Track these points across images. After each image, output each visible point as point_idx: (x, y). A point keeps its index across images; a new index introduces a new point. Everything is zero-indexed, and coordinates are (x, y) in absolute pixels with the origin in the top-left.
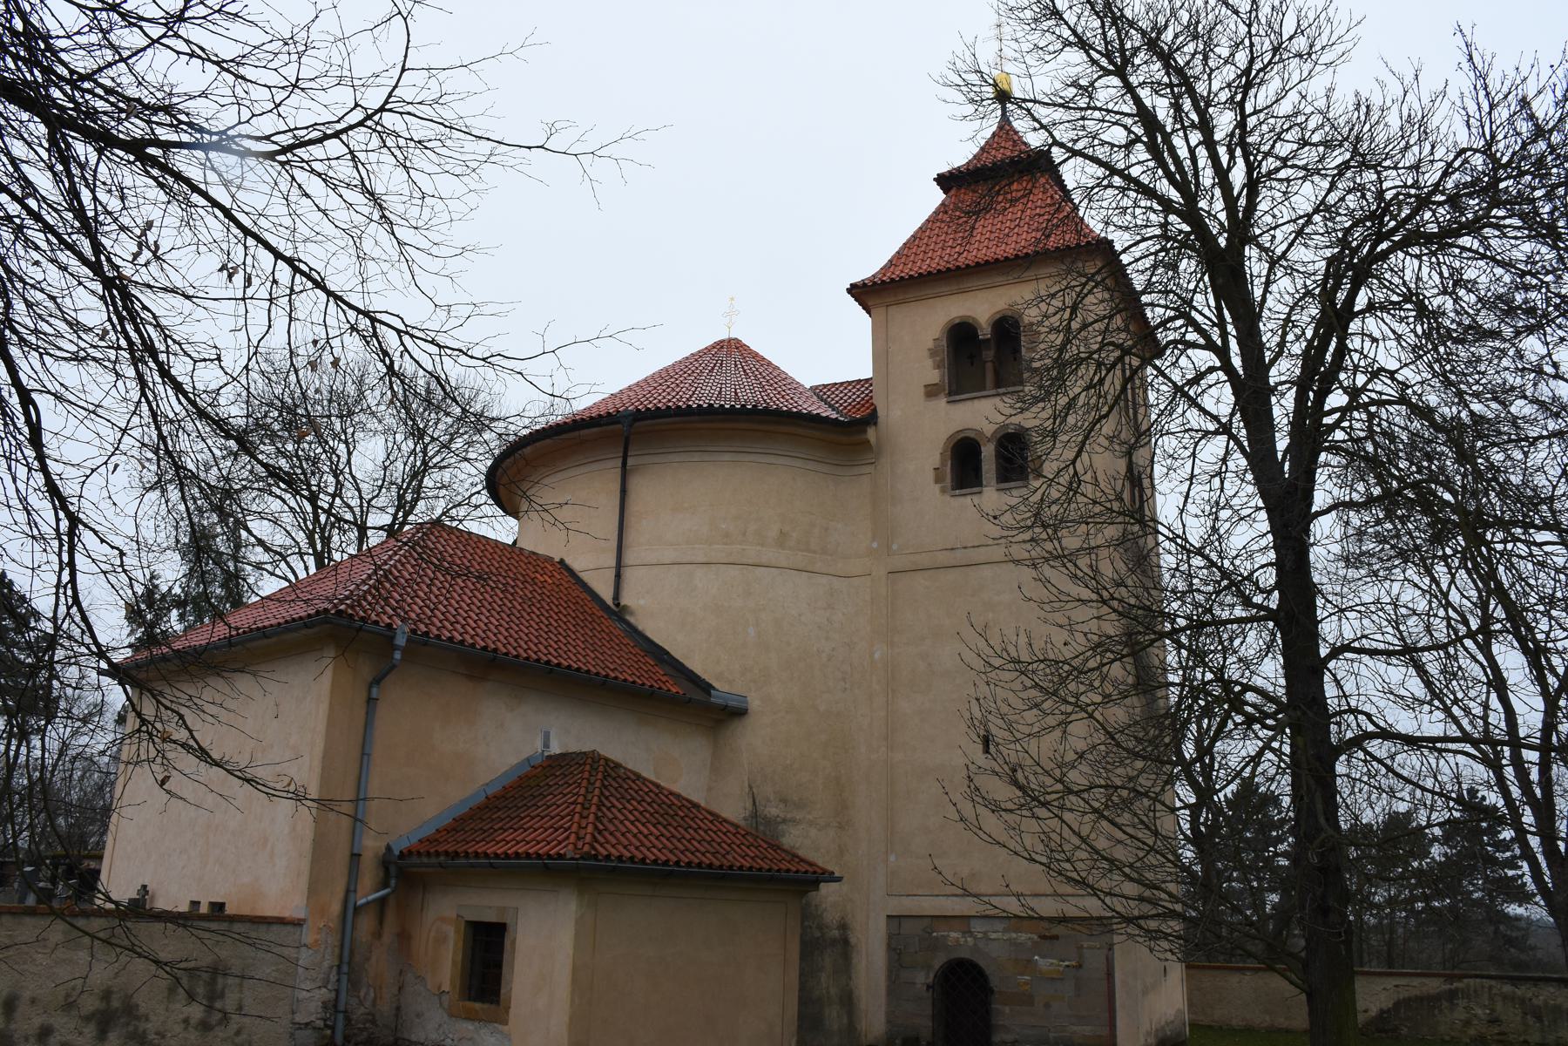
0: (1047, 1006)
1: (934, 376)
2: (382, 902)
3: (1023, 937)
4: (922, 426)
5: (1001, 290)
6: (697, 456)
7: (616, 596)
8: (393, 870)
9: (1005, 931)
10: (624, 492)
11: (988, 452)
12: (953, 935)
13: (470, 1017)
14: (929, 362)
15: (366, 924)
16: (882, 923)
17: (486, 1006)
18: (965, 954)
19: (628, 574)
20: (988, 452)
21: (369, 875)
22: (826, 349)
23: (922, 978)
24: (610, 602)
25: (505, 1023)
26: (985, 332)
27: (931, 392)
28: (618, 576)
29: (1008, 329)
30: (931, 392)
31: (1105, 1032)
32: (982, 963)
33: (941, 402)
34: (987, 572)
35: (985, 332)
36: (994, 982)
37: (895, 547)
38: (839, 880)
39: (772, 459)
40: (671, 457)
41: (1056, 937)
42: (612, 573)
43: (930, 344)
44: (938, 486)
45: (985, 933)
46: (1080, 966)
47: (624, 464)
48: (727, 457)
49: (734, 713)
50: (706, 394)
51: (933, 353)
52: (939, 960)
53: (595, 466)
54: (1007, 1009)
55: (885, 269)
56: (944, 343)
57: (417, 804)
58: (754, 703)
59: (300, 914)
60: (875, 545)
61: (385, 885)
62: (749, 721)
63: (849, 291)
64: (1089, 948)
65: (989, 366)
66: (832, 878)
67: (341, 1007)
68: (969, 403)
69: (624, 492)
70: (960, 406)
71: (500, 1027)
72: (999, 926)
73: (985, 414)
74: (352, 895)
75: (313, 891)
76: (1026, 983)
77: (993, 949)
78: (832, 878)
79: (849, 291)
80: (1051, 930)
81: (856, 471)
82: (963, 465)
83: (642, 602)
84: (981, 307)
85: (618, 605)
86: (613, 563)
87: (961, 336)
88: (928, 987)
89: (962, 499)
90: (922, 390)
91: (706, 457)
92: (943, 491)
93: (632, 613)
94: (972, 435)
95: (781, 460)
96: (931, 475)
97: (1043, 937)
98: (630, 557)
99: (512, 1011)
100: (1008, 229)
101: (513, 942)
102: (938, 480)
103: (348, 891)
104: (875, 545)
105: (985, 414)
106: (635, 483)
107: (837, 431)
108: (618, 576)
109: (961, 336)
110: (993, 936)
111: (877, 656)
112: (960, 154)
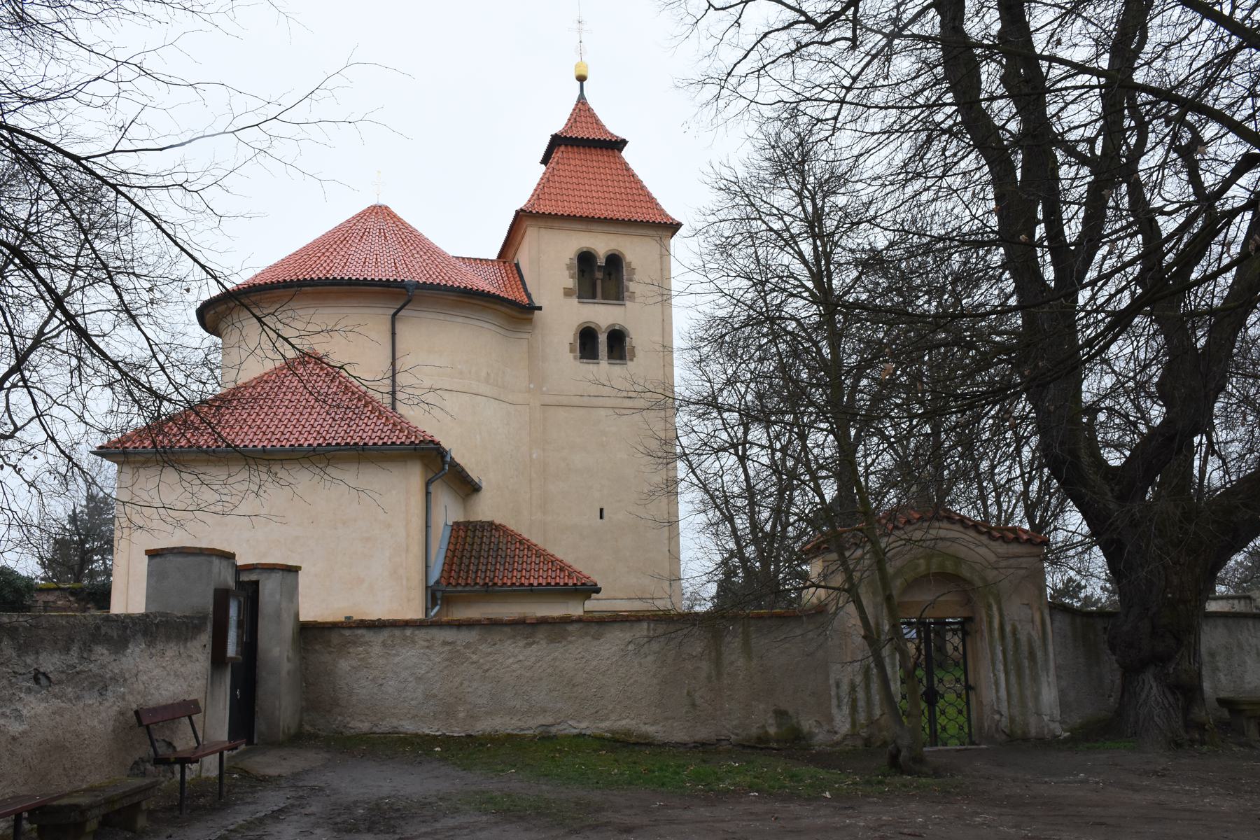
1: (571, 283)
4: (562, 313)
5: (611, 236)
6: (442, 317)
8: (439, 595)
10: (394, 334)
11: (603, 338)
20: (603, 338)
26: (601, 261)
27: (568, 293)
29: (615, 261)
30: (568, 293)
33: (574, 301)
34: (602, 412)
40: (424, 314)
43: (568, 261)
47: (394, 315)
48: (460, 320)
51: (569, 267)
58: (484, 485)
69: (394, 334)
73: (603, 315)
78: (598, 591)
82: (587, 341)
84: (601, 244)
87: (585, 260)
91: (448, 318)
92: (575, 358)
95: (486, 325)
96: (567, 348)
105: (603, 315)
106: (400, 328)
109: (585, 260)
111: (534, 456)
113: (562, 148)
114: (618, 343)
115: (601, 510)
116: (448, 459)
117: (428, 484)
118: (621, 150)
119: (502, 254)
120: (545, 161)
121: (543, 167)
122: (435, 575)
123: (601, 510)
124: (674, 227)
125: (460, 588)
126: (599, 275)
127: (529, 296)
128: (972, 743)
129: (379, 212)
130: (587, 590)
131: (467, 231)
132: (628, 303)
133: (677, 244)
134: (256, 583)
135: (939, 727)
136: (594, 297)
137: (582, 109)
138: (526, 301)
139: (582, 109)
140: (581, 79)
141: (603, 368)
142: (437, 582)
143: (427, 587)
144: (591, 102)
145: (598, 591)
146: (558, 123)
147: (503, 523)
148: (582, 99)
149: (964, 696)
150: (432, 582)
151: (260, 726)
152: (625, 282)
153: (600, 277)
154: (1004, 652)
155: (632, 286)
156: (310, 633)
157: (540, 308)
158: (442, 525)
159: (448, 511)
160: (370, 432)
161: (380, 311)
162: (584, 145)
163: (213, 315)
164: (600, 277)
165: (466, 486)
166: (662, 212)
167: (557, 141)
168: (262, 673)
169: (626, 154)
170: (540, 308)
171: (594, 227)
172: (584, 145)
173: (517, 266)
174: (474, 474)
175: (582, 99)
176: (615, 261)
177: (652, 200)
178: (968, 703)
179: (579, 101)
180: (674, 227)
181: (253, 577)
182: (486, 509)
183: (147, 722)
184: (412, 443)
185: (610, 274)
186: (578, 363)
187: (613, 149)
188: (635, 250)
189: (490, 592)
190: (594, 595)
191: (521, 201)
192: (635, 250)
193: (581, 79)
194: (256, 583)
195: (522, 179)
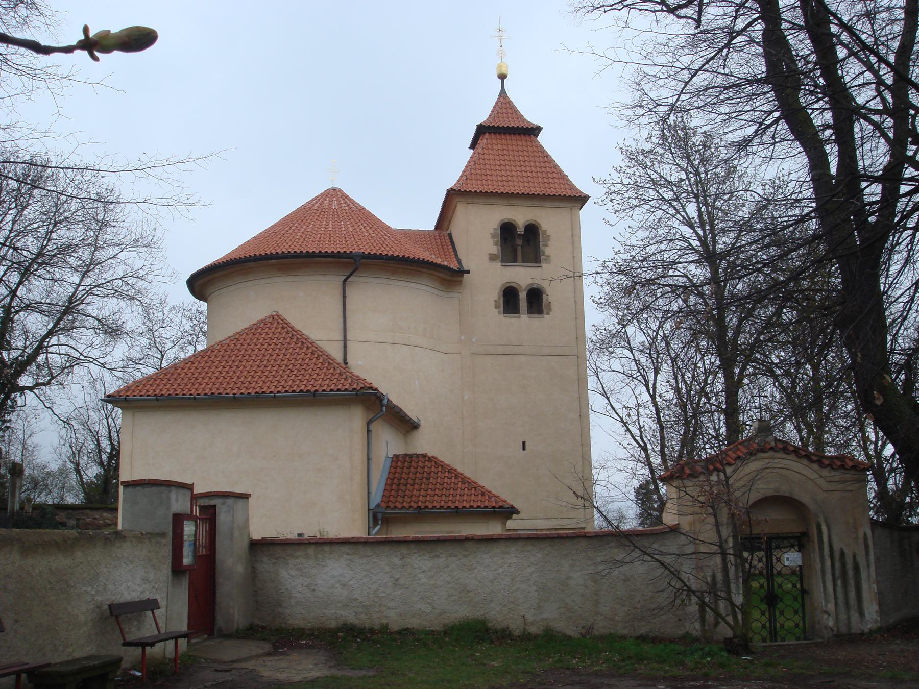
1: (495, 250)
4: (487, 274)
5: (529, 209)
6: (385, 281)
8: (380, 516)
10: (344, 297)
11: (523, 296)
14: (491, 241)
20: (523, 296)
26: (521, 230)
27: (492, 258)
28: (345, 347)
29: (532, 230)
30: (492, 258)
33: (498, 264)
34: (523, 358)
43: (492, 231)
47: (345, 280)
51: (493, 236)
53: (322, 278)
58: (422, 423)
62: (421, 430)
69: (344, 297)
73: (523, 276)
78: (517, 512)
81: (451, 295)
82: (510, 299)
83: (360, 363)
84: (521, 216)
85: (346, 363)
86: (342, 338)
87: (507, 229)
92: (499, 313)
94: (514, 285)
98: (349, 337)
102: (497, 307)
104: (463, 338)
105: (523, 276)
108: (345, 347)
109: (507, 229)
111: (466, 397)
113: (487, 135)
114: (536, 300)
115: (524, 443)
116: (385, 402)
117: (369, 423)
118: (537, 135)
119: (438, 227)
120: (473, 146)
121: (472, 151)
122: (377, 498)
123: (524, 443)
124: (582, 200)
125: (397, 511)
126: (519, 242)
127: (459, 261)
128: (806, 638)
129: (334, 194)
130: (508, 512)
131: (407, 207)
132: (544, 265)
133: (586, 213)
134: (214, 507)
135: (778, 625)
136: (515, 260)
137: (504, 103)
138: (454, 265)
139: (504, 103)
140: (502, 77)
141: (524, 320)
142: (378, 506)
143: (369, 510)
144: (512, 96)
145: (517, 512)
146: (483, 116)
147: (435, 455)
148: (503, 93)
149: (800, 600)
150: (373, 506)
151: (220, 622)
152: (542, 248)
153: (521, 243)
154: (833, 565)
155: (548, 251)
156: (258, 547)
157: (468, 272)
158: (383, 458)
159: (389, 443)
160: (322, 383)
161: (333, 278)
162: (506, 132)
163: (202, 283)
164: (521, 243)
165: (405, 424)
166: (572, 187)
167: (482, 130)
168: (220, 580)
169: (541, 138)
170: (468, 272)
172: (506, 132)
173: (450, 235)
174: (412, 412)
175: (503, 93)
176: (532, 230)
177: (564, 177)
178: (803, 605)
179: (500, 95)
180: (582, 200)
181: (212, 502)
182: (424, 443)
183: (119, 613)
184: (354, 389)
185: (528, 241)
187: (530, 135)
188: (548, 220)
189: (421, 515)
190: (514, 516)
191: (451, 179)
192: (548, 220)
193: (502, 77)
194: (214, 507)
195: (453, 161)
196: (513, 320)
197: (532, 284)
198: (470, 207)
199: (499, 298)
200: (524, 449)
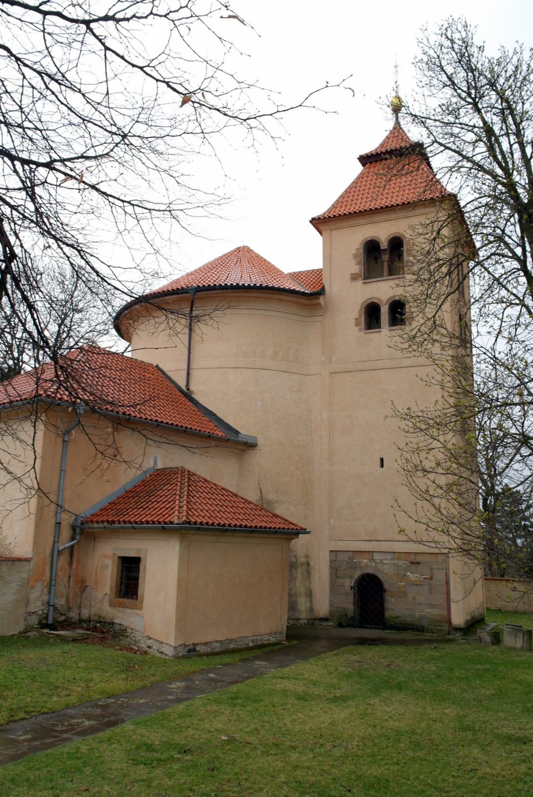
0: (414, 598)
1: (357, 269)
2: (72, 547)
3: (401, 563)
4: (350, 295)
7: (187, 385)
8: (78, 530)
9: (393, 559)
12: (365, 561)
13: (121, 605)
14: (353, 261)
15: (63, 560)
16: (327, 555)
17: (130, 600)
18: (371, 571)
19: (193, 373)
21: (66, 533)
22: (297, 252)
23: (348, 583)
24: (184, 388)
25: (141, 609)
26: (384, 245)
27: (354, 278)
29: (396, 244)
30: (354, 278)
31: (445, 613)
32: (380, 576)
33: (360, 283)
34: (382, 373)
35: (384, 245)
36: (386, 586)
37: (334, 360)
38: (309, 533)
39: (269, 313)
41: (419, 563)
42: (185, 372)
43: (354, 252)
44: (357, 328)
45: (381, 560)
46: (431, 578)
48: (246, 311)
49: (250, 445)
50: (234, 279)
51: (355, 256)
52: (358, 574)
54: (393, 600)
55: (329, 210)
56: (362, 251)
57: (92, 494)
58: (260, 441)
59: (29, 555)
60: (323, 358)
61: (73, 539)
63: (311, 222)
64: (436, 569)
65: (386, 264)
66: (304, 531)
67: (51, 603)
68: (374, 284)
70: (370, 285)
71: (136, 611)
72: (389, 557)
73: (384, 290)
74: (56, 544)
75: (36, 544)
76: (403, 587)
77: (386, 571)
78: (304, 531)
79: (311, 222)
80: (414, 560)
82: (372, 315)
83: (201, 388)
84: (382, 231)
85: (188, 389)
86: (185, 367)
87: (371, 248)
88: (352, 588)
89: (370, 335)
90: (349, 277)
92: (360, 330)
93: (195, 394)
94: (376, 301)
95: (274, 314)
96: (353, 322)
97: (412, 563)
98: (194, 365)
99: (144, 603)
100: (403, 188)
101: (145, 567)
102: (357, 324)
103: (54, 542)
104: (323, 358)
105: (384, 290)
107: (305, 297)
108: (188, 374)
109: (371, 248)
110: (386, 562)
111: (324, 416)
112: (371, 145)
115: (382, 460)
123: (382, 460)
141: (385, 334)
148: (398, 126)
171: (377, 218)
186: (362, 333)
196: (373, 335)
197: (394, 296)
198: (334, 232)
199: (360, 316)
200: (382, 466)
